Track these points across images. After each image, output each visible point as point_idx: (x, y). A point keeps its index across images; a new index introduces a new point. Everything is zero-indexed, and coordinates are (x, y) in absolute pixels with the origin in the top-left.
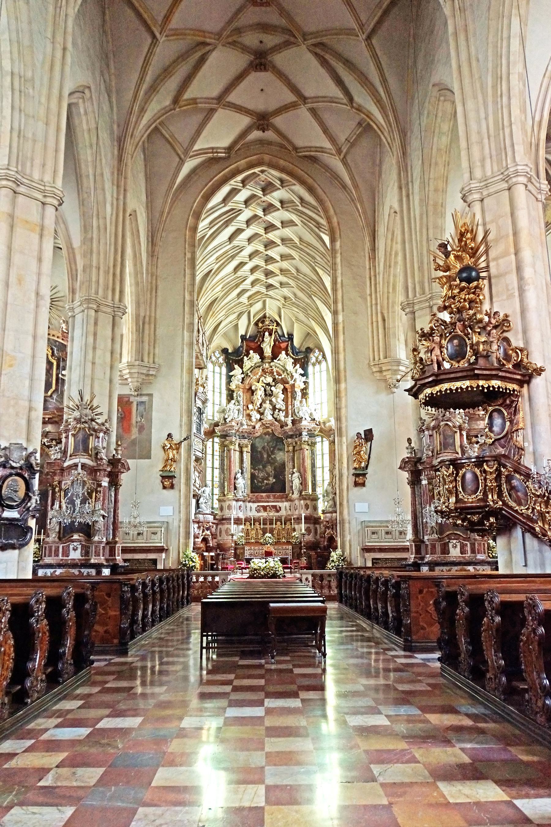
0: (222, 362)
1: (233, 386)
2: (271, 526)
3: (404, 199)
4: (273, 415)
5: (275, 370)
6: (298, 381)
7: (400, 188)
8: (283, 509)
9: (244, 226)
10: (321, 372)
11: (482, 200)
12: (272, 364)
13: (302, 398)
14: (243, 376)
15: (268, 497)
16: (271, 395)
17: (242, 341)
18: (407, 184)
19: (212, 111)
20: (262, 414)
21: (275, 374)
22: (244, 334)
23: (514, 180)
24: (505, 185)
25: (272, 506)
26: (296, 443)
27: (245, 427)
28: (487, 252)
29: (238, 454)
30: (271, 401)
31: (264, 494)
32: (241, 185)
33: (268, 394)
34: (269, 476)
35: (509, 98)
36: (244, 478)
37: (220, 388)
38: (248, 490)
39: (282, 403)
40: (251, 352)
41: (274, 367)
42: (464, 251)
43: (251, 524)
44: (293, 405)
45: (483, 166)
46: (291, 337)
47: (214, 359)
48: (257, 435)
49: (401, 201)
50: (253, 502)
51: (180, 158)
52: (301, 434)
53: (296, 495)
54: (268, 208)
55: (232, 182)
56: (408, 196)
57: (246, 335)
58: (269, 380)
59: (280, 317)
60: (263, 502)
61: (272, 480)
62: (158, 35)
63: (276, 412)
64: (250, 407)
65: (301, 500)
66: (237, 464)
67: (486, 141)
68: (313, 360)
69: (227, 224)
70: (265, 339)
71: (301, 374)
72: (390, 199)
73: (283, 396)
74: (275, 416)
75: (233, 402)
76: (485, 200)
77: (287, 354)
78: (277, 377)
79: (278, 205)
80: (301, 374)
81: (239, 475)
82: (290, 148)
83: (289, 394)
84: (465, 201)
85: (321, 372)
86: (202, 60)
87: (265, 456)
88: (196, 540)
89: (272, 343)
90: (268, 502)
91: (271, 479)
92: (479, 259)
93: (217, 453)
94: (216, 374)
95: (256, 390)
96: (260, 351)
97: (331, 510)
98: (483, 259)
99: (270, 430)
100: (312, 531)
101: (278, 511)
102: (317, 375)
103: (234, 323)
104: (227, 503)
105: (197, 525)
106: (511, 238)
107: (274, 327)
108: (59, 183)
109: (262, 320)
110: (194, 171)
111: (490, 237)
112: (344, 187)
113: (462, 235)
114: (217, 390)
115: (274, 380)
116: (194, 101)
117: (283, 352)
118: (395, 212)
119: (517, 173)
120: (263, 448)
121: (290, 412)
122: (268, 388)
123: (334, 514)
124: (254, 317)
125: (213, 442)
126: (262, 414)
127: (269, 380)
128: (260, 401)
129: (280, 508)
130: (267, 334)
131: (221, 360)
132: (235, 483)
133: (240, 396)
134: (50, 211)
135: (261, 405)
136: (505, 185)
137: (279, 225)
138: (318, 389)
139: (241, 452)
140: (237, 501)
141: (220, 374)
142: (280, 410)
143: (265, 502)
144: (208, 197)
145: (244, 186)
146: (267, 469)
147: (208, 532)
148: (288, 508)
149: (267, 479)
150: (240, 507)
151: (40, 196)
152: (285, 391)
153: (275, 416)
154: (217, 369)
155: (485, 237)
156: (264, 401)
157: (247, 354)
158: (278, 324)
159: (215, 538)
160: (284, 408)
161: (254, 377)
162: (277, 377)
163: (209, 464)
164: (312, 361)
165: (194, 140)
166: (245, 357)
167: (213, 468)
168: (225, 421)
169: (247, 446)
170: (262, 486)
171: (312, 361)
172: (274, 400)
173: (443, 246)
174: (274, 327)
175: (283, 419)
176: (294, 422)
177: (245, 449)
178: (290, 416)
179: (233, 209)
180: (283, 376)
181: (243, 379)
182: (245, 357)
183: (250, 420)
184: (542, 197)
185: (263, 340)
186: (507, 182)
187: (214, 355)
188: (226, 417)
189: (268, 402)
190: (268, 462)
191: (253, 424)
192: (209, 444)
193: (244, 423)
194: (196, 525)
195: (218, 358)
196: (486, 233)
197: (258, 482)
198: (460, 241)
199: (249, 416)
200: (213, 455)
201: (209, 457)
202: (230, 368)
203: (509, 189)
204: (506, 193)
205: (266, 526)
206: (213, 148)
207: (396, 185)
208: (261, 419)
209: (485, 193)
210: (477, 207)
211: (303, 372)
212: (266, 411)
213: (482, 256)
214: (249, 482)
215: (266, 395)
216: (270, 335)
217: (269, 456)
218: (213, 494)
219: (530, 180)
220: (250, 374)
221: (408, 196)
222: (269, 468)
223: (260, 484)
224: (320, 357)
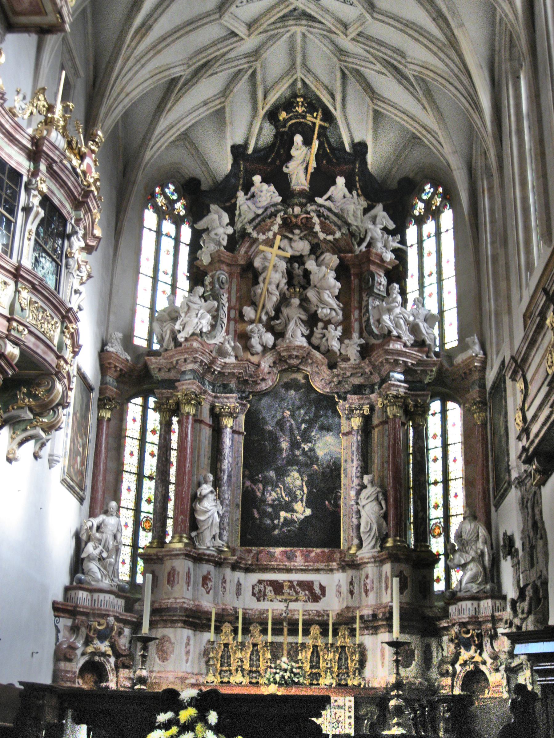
0: (183, 213)
1: (205, 259)
2: (291, 639)
4: (308, 338)
5: (316, 220)
6: (379, 245)
8: (331, 592)
10: (438, 234)
12: (310, 208)
13: (389, 283)
14: (230, 230)
15: (290, 557)
16: (304, 288)
17: (235, 164)
20: (279, 335)
21: (317, 228)
22: (240, 141)
25: (301, 583)
26: (372, 408)
27: (231, 360)
29: (206, 433)
30: (304, 300)
31: (278, 551)
33: (298, 279)
34: (294, 499)
36: (219, 497)
37: (174, 276)
38: (232, 536)
39: (334, 303)
40: (257, 179)
41: (312, 214)
43: (235, 631)
44: (364, 310)
46: (360, 148)
47: (160, 201)
48: (264, 386)
50: (248, 570)
52: (385, 379)
53: (367, 552)
57: (245, 146)
58: (302, 247)
59: (333, 96)
60: (274, 570)
61: (302, 511)
63: (318, 331)
64: (249, 312)
65: (382, 562)
66: (205, 461)
68: (420, 208)
70: (293, 152)
71: (385, 229)
73: (339, 285)
74: (315, 341)
75: (200, 290)
77: (350, 186)
78: (322, 236)
80: (385, 229)
81: (206, 488)
83: (355, 282)
85: (438, 234)
87: (285, 445)
88: (63, 665)
89: (313, 164)
90: (288, 571)
91: (298, 506)
93: (153, 439)
94: (164, 239)
95: (265, 269)
96: (281, 182)
97: (474, 588)
99: (299, 377)
100: (417, 654)
101: (316, 599)
102: (430, 245)
103: (214, 106)
104: (168, 564)
105: (69, 622)
107: (318, 122)
109: (288, 104)
114: (165, 278)
115: (316, 250)
117: (341, 181)
120: (281, 424)
121: (356, 325)
122: (298, 271)
123: (487, 604)
124: (265, 97)
125: (145, 407)
126: (279, 335)
127: (302, 247)
128: (275, 299)
129: (323, 589)
130: (298, 139)
131: (180, 207)
132: (193, 511)
133: (221, 283)
135: (278, 310)
138: (431, 281)
139: (217, 432)
140: (198, 559)
141: (177, 240)
142: (327, 323)
143: (280, 570)
146: (288, 480)
147: (104, 647)
148: (345, 588)
149: (289, 508)
150: (206, 579)
152: (342, 272)
153: (315, 341)
154: (168, 227)
156: (284, 300)
157: (248, 186)
158: (328, 117)
159: (125, 667)
160: (340, 317)
161: (262, 237)
162: (322, 236)
163: (130, 463)
164: (416, 213)
166: (241, 194)
167: (140, 476)
168: (175, 339)
169: (232, 415)
170: (275, 527)
171: (416, 213)
172: (311, 294)
174: (318, 122)
175: (335, 345)
176: (365, 351)
177: (228, 422)
178: (355, 335)
180: (338, 235)
181: (231, 238)
182: (241, 194)
183: (247, 348)
185: (290, 158)
187: (163, 193)
188: (177, 327)
189: (296, 301)
190: (292, 461)
191: (255, 359)
192: (134, 408)
193: (228, 347)
194: (65, 622)
195: (171, 203)
197: (264, 514)
199: (244, 338)
200: (143, 441)
201: (131, 446)
202: (196, 212)
205: (279, 639)
208: (274, 345)
211: (391, 226)
212: (292, 326)
214: (238, 514)
215: (290, 283)
216: (307, 142)
217: (295, 445)
218: (135, 546)
220: (250, 230)
222: (295, 479)
223: (268, 522)
224: (438, 201)
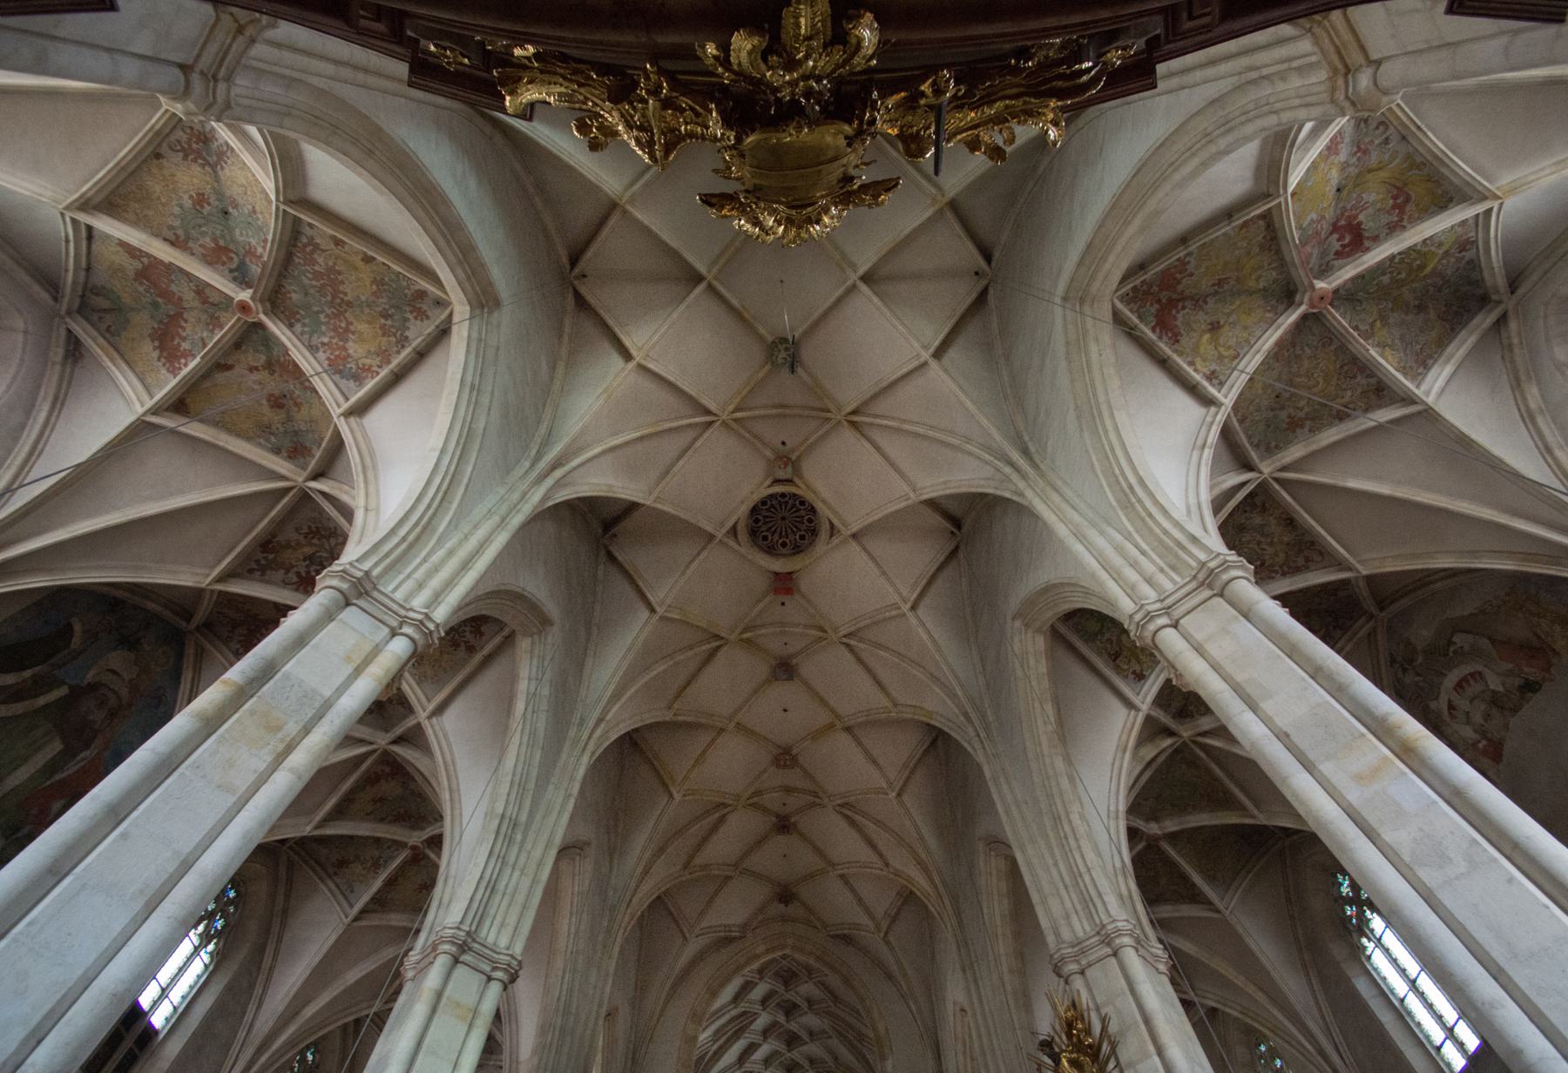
3: (972, 987)
7: (964, 971)
9: (757, 1039)
11: (1082, 973)
19: (728, 878)
23: (1118, 941)
24: (1108, 950)
28: (1113, 1051)
35: (1077, 840)
42: (1078, 1052)
45: (1070, 925)
49: (968, 989)
51: (685, 938)
54: (790, 1009)
55: (746, 971)
56: (976, 981)
62: (675, 795)
67: (1063, 892)
69: (737, 1035)
72: (955, 991)
76: (1088, 973)
79: (805, 1005)
84: (1059, 976)
86: (722, 820)
92: (1107, 1063)
98: (1111, 1065)
106: (1143, 1027)
108: (518, 949)
110: (700, 957)
111: (1113, 1028)
112: (889, 976)
113: (1070, 1025)
116: (705, 867)
118: (962, 1010)
119: (1119, 933)
134: (495, 989)
136: (1108, 950)
137: (805, 1036)
144: (714, 994)
151: (487, 968)
155: (1104, 1029)
165: (702, 914)
173: (1047, 1045)
179: (745, 1013)
184: (1162, 967)
186: (1109, 944)
196: (1104, 1021)
198: (1069, 1035)
203: (1115, 954)
204: (1113, 960)
207: (958, 966)
209: (1084, 962)
210: (1078, 983)
213: (1108, 1059)
219: (1138, 941)
221: (976, 981)
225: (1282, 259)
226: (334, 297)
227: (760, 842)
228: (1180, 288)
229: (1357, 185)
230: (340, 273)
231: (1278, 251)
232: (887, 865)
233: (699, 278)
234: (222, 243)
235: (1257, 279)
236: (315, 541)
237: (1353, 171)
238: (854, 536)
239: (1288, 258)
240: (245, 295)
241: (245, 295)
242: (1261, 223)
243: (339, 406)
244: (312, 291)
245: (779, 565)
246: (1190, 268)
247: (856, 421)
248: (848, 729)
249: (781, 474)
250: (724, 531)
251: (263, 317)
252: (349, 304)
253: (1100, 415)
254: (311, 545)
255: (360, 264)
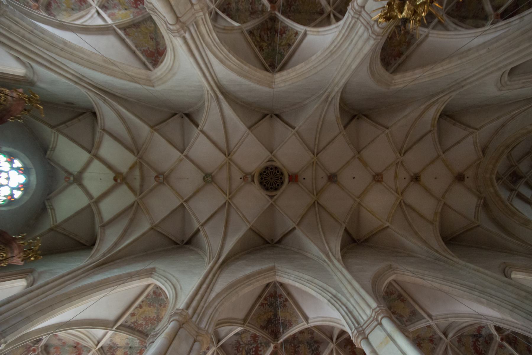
3: (468, 81)
18: (459, 83)
32: (514, 192)
51: (478, 226)
56: (465, 80)
62: (386, 225)
67: (354, 42)
82: (478, 162)
145: (516, 190)
206: (476, 207)
221: (465, 80)
225: (143, 21)
226: (155, 320)
227: (426, 189)
228: (153, 51)
229: (124, 5)
230: (146, 317)
231: (139, 23)
232: (430, 131)
233: (182, 204)
234: (139, 351)
235: (150, 27)
236: (241, 349)
237: (120, 7)
238: (271, 153)
239: (141, 19)
240: (272, 346)
241: (272, 346)
242: (127, 30)
243: (304, 325)
244: (153, 327)
245: (287, 180)
246: (146, 49)
247: (228, 153)
248: (359, 152)
249: (250, 179)
250: (270, 200)
251: (279, 342)
252: (158, 316)
253: (302, 72)
254: (242, 351)
255: (142, 310)
